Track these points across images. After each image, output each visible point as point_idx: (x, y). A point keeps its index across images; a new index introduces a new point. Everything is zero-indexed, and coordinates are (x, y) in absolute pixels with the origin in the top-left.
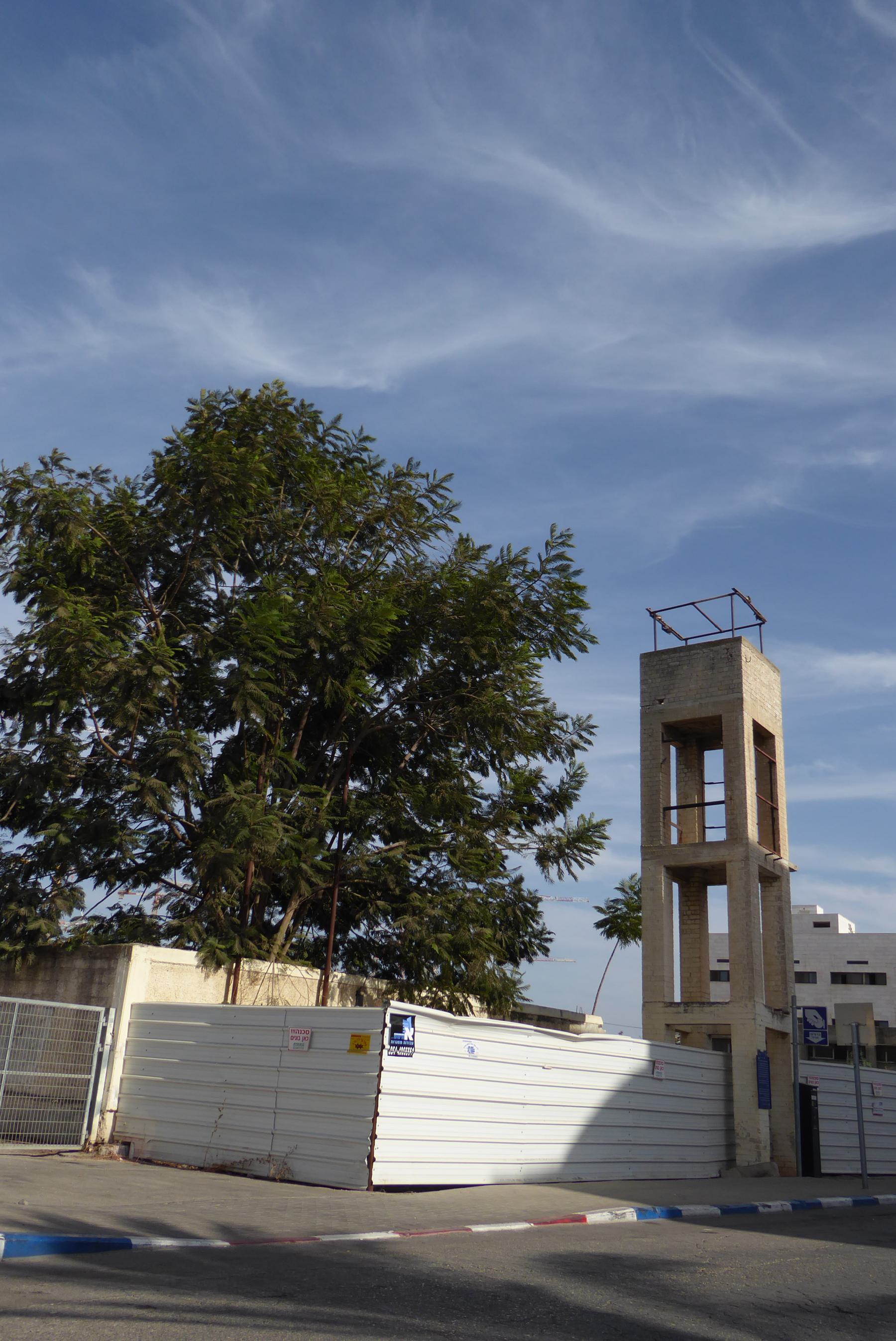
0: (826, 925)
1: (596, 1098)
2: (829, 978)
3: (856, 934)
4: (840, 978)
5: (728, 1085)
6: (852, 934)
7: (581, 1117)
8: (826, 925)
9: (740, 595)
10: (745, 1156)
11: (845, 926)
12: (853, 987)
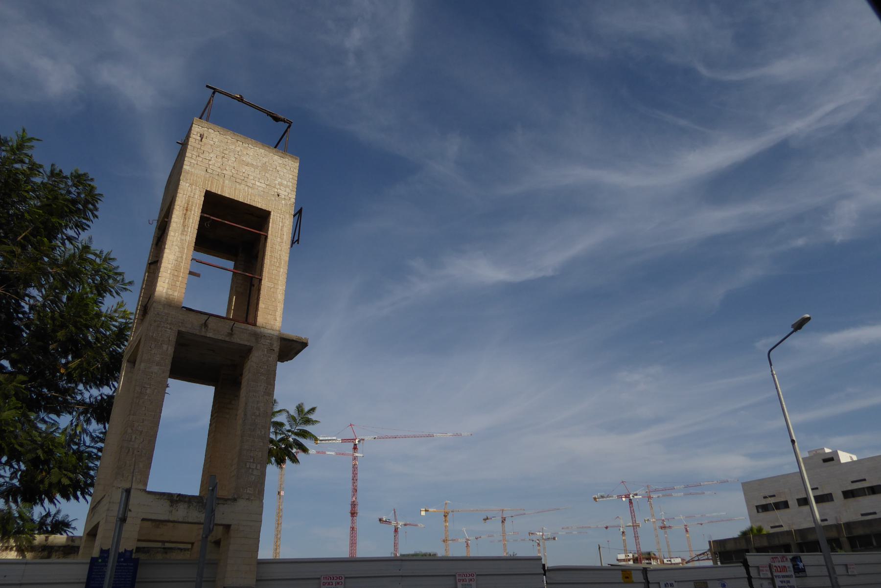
0: (832, 459)
2: (841, 496)
3: (859, 461)
4: (848, 494)
6: (853, 462)
8: (832, 459)
9: (221, 92)
11: (845, 457)
12: (861, 499)
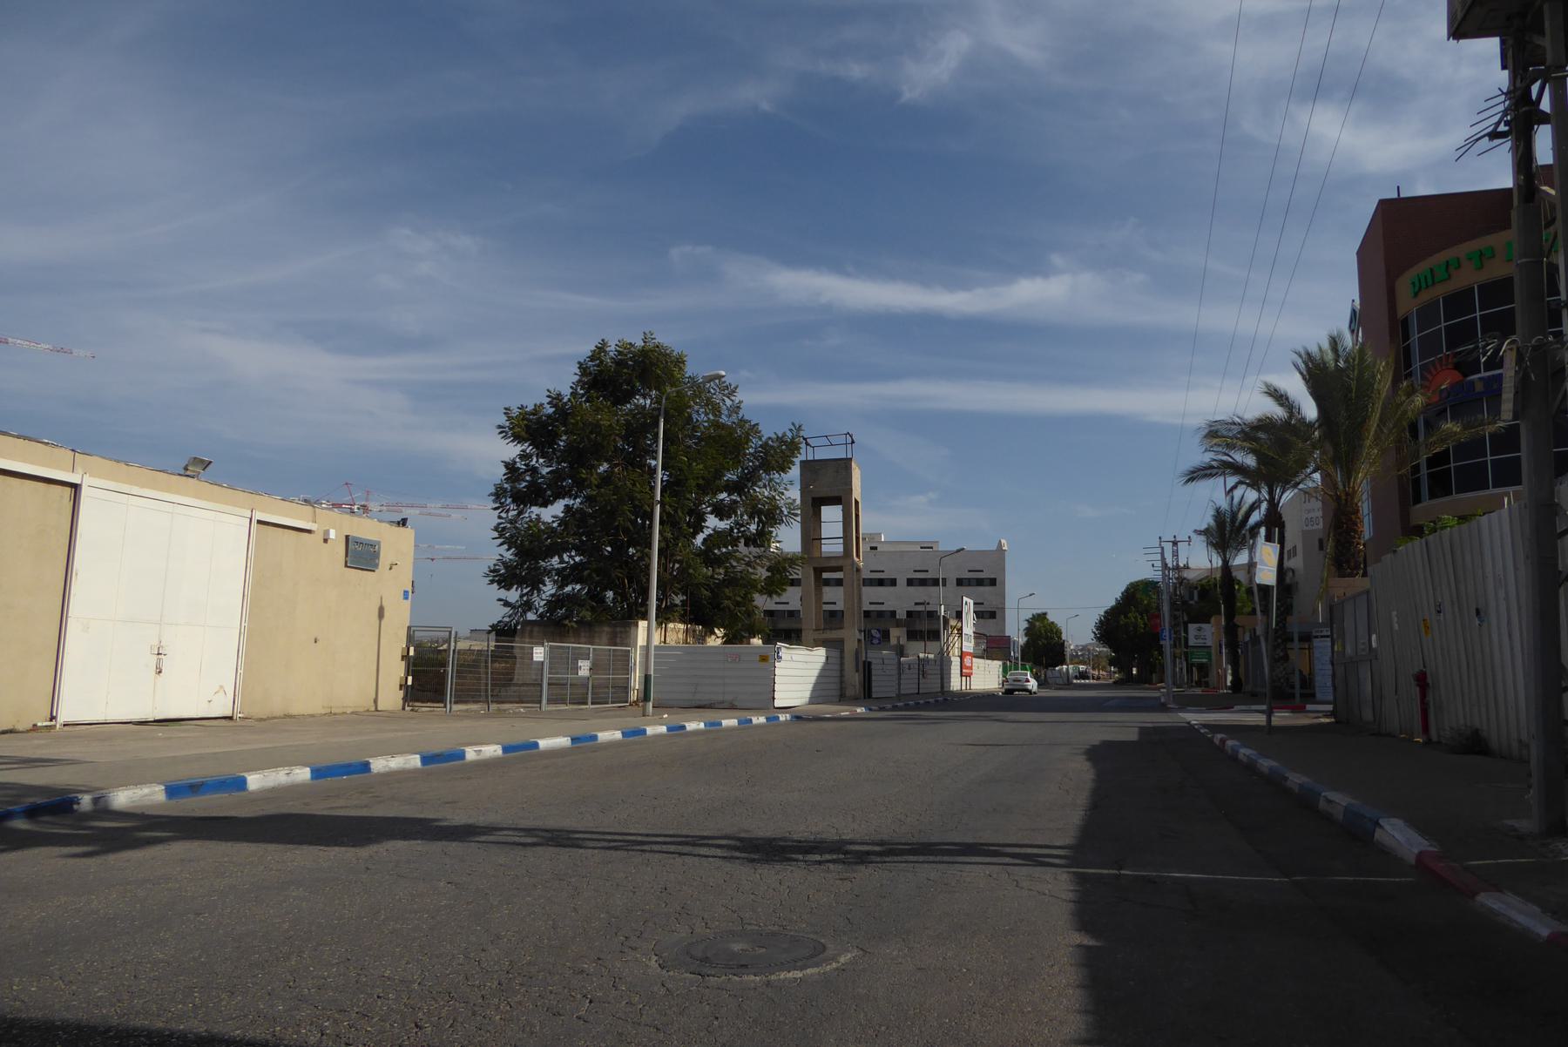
1: (816, 673)
5: (842, 664)
7: (813, 680)
10: (850, 692)
